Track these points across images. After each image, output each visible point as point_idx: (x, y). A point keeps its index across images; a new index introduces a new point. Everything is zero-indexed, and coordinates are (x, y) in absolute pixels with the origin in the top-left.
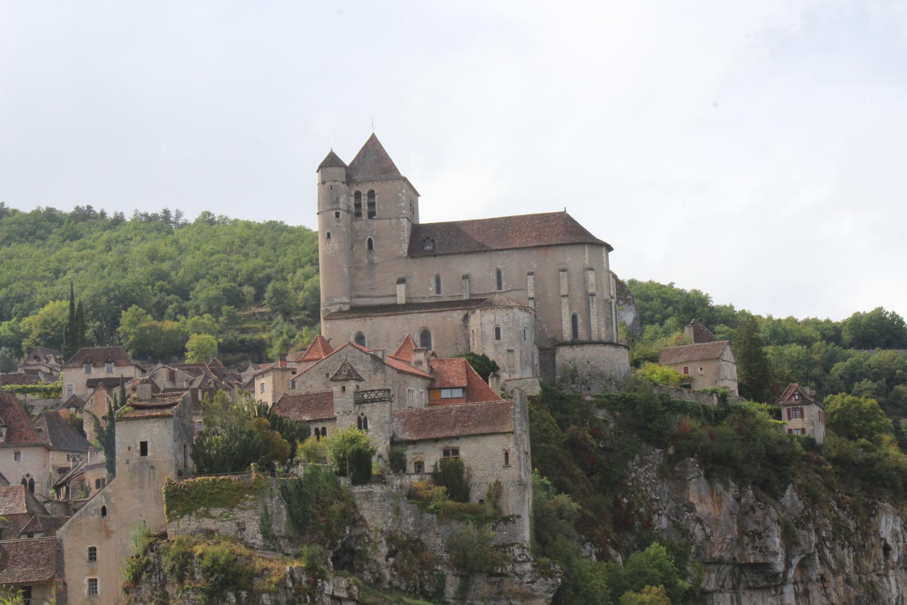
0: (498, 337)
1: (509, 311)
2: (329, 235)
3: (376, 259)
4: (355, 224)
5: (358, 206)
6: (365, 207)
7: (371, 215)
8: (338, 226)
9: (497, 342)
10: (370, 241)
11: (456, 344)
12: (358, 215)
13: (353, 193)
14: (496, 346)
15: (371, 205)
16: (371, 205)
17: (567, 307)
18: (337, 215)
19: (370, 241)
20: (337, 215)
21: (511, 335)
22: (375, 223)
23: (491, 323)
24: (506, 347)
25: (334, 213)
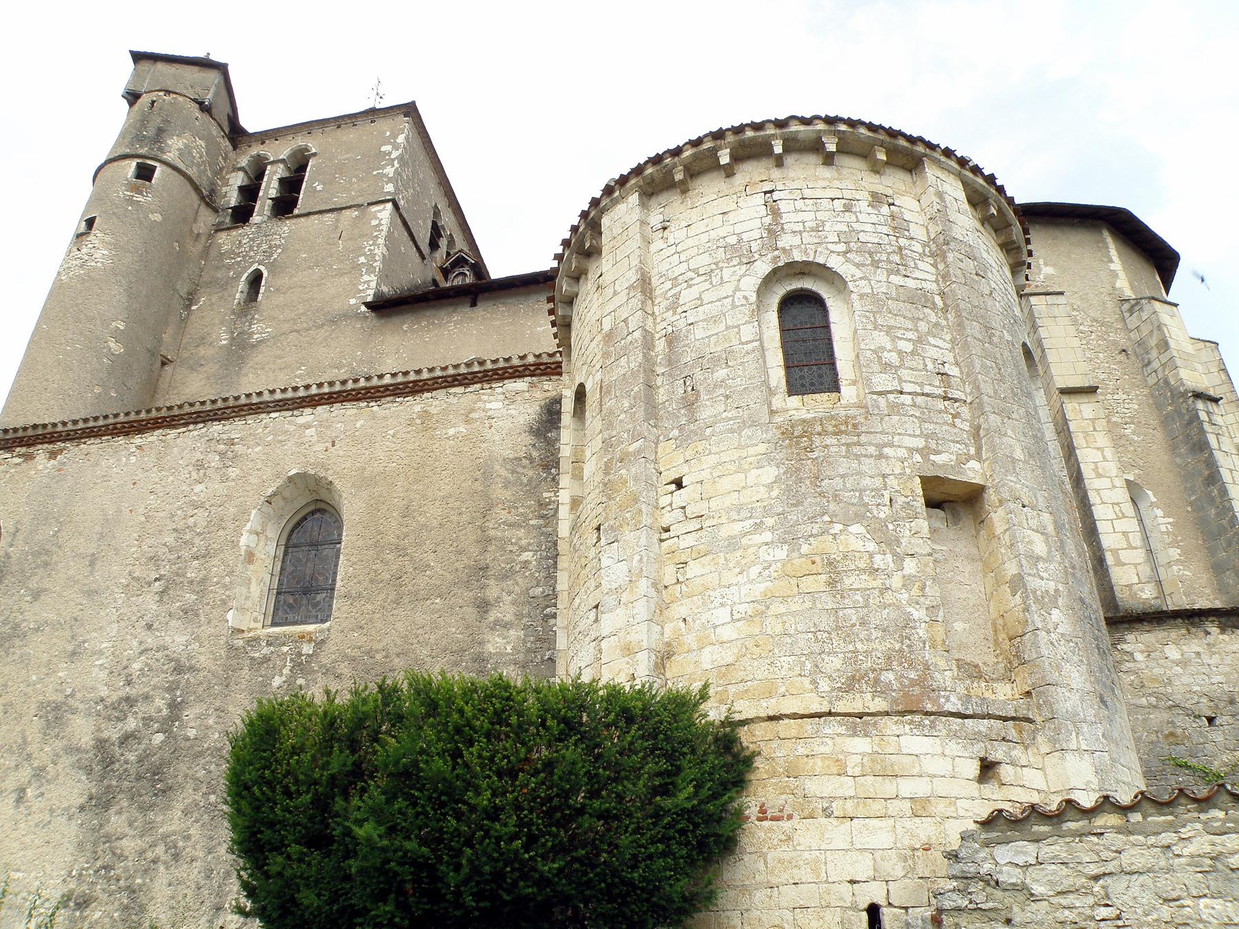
0: (811, 364)
1: (894, 182)
2: (90, 223)
3: (259, 329)
4: (222, 237)
5: (250, 193)
6: (270, 188)
7: (285, 206)
8: (130, 201)
9: (813, 406)
10: (256, 279)
11: (482, 570)
12: (242, 215)
13: (244, 161)
14: (796, 437)
15: (291, 185)
16: (291, 185)
17: (1102, 440)
18: (145, 173)
19: (256, 279)
20: (145, 173)
21: (939, 349)
22: (287, 227)
23: (741, 254)
24: (901, 455)
25: (132, 165)
